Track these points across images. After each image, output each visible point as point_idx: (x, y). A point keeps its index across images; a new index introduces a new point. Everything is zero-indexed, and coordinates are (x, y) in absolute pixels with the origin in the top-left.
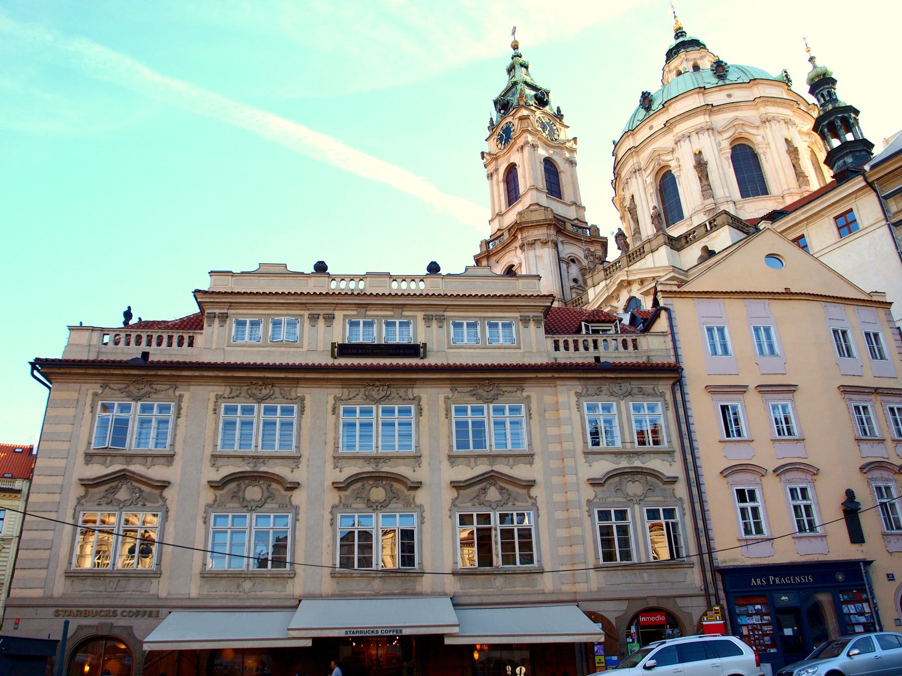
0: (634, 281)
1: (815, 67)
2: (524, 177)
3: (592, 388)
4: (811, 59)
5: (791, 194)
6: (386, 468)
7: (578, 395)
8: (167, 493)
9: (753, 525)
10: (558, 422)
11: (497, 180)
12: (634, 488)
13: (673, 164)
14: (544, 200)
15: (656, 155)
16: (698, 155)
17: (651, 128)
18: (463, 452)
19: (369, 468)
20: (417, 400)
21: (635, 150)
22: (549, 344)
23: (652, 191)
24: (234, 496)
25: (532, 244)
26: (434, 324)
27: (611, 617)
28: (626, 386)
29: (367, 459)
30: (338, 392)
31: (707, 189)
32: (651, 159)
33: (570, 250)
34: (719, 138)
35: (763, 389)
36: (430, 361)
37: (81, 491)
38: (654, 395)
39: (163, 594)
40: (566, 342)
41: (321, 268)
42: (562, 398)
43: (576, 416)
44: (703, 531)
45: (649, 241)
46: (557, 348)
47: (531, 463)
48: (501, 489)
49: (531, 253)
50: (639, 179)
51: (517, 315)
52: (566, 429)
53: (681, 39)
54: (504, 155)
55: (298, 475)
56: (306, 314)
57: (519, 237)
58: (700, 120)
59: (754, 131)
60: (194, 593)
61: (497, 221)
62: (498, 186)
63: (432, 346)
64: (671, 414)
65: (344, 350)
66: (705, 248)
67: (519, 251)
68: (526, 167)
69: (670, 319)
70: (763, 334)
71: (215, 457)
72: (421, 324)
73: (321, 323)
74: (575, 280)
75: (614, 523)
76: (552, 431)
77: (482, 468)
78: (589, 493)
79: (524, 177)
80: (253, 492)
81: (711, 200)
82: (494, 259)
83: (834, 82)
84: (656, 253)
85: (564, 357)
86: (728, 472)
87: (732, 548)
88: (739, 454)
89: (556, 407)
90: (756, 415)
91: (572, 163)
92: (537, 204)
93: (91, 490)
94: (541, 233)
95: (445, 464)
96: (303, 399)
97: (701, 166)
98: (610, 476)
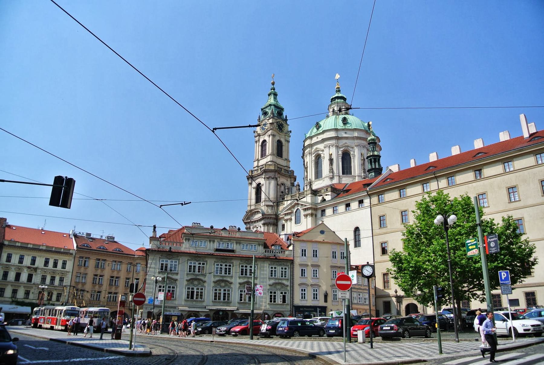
3: (273, 263)
6: (225, 279)
7: (269, 265)
9: (303, 297)
12: (279, 287)
13: (322, 155)
15: (317, 150)
19: (221, 278)
20: (233, 263)
21: (311, 146)
27: (270, 314)
28: (280, 263)
31: (331, 170)
33: (282, 180)
35: (312, 265)
36: (237, 254)
38: (286, 266)
41: (212, 227)
42: (265, 265)
44: (292, 298)
52: (265, 272)
58: (333, 142)
59: (351, 149)
64: (289, 270)
65: (217, 250)
67: (263, 179)
69: (293, 247)
72: (235, 245)
73: (212, 243)
75: (273, 294)
76: (262, 272)
77: (246, 280)
78: (268, 287)
85: (267, 254)
86: (300, 285)
87: (298, 301)
88: (303, 281)
90: (309, 272)
91: (288, 142)
95: (238, 278)
97: (331, 160)
98: (274, 284)
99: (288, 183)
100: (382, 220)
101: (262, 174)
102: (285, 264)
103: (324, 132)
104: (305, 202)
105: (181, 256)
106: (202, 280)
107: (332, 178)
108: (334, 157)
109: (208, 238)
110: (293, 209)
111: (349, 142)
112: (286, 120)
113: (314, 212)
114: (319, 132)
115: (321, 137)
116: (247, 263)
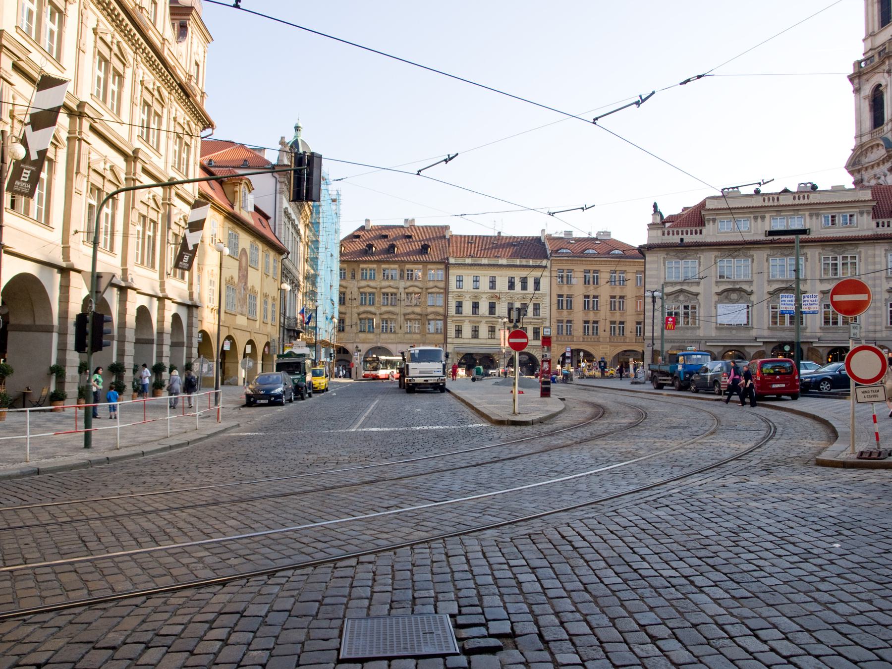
7: (886, 250)
8: (699, 297)
10: (874, 263)
18: (826, 277)
19: (784, 285)
22: (874, 224)
24: (726, 298)
26: (814, 217)
29: (783, 281)
30: (768, 252)
36: (812, 236)
39: (702, 335)
40: (883, 223)
42: (877, 252)
43: (884, 260)
46: (878, 226)
55: (754, 288)
56: (752, 216)
60: (714, 335)
63: (814, 229)
65: (771, 233)
71: (717, 282)
72: (808, 218)
73: (759, 220)
78: (887, 295)
80: (734, 296)
85: (881, 231)
89: (874, 256)
96: (753, 256)
106: (745, 291)
116: (836, 252)
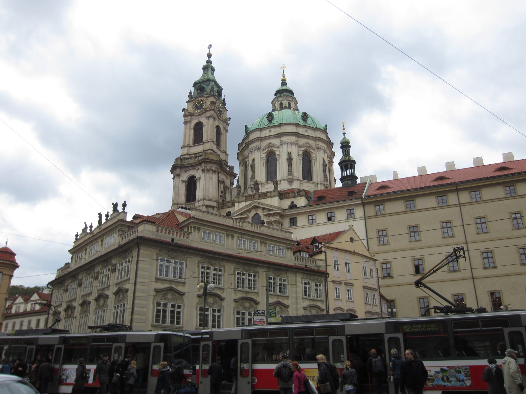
0: (260, 207)
1: (345, 137)
2: (207, 133)
4: (344, 134)
5: (321, 184)
6: (249, 296)
7: (302, 278)
11: (190, 127)
13: (277, 153)
14: (214, 147)
16: (289, 154)
17: (270, 131)
21: (260, 139)
23: (264, 161)
25: (208, 171)
31: (290, 171)
32: (268, 146)
33: (222, 177)
34: (299, 149)
37: (155, 293)
45: (271, 192)
47: (288, 299)
48: (280, 307)
49: (208, 175)
50: (259, 153)
51: (286, 246)
53: (284, 87)
54: (197, 116)
57: (203, 165)
58: (293, 138)
61: (186, 149)
62: (190, 130)
66: (292, 203)
67: (200, 171)
68: (209, 128)
69: (326, 256)
70: (347, 264)
72: (259, 244)
74: (222, 192)
79: (207, 133)
81: (290, 177)
82: (184, 169)
83: (350, 147)
84: (273, 199)
91: (227, 131)
92: (212, 150)
93: (158, 293)
94: (214, 167)
97: (290, 160)
99: (228, 182)
100: (382, 234)
101: (200, 164)
102: (319, 278)
103: (280, 125)
104: (267, 205)
105: (190, 254)
107: (291, 182)
108: (294, 156)
109: (226, 230)
110: (248, 214)
111: (312, 143)
112: (224, 103)
113: (281, 220)
114: (272, 125)
115: (275, 131)
